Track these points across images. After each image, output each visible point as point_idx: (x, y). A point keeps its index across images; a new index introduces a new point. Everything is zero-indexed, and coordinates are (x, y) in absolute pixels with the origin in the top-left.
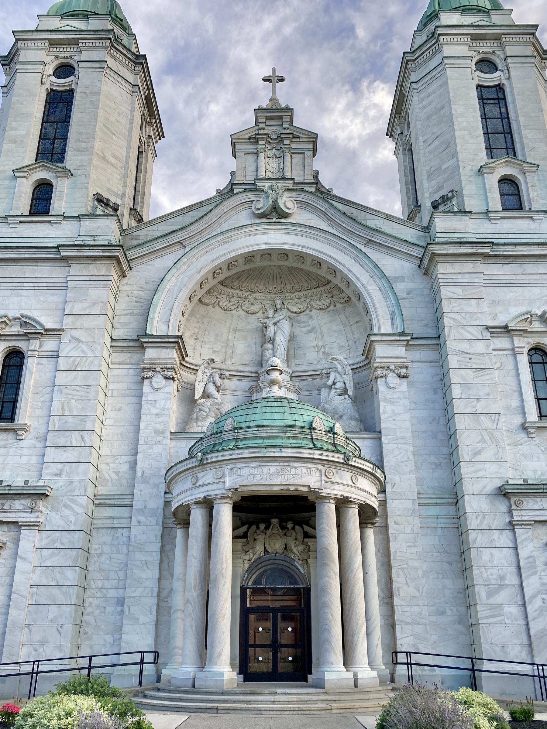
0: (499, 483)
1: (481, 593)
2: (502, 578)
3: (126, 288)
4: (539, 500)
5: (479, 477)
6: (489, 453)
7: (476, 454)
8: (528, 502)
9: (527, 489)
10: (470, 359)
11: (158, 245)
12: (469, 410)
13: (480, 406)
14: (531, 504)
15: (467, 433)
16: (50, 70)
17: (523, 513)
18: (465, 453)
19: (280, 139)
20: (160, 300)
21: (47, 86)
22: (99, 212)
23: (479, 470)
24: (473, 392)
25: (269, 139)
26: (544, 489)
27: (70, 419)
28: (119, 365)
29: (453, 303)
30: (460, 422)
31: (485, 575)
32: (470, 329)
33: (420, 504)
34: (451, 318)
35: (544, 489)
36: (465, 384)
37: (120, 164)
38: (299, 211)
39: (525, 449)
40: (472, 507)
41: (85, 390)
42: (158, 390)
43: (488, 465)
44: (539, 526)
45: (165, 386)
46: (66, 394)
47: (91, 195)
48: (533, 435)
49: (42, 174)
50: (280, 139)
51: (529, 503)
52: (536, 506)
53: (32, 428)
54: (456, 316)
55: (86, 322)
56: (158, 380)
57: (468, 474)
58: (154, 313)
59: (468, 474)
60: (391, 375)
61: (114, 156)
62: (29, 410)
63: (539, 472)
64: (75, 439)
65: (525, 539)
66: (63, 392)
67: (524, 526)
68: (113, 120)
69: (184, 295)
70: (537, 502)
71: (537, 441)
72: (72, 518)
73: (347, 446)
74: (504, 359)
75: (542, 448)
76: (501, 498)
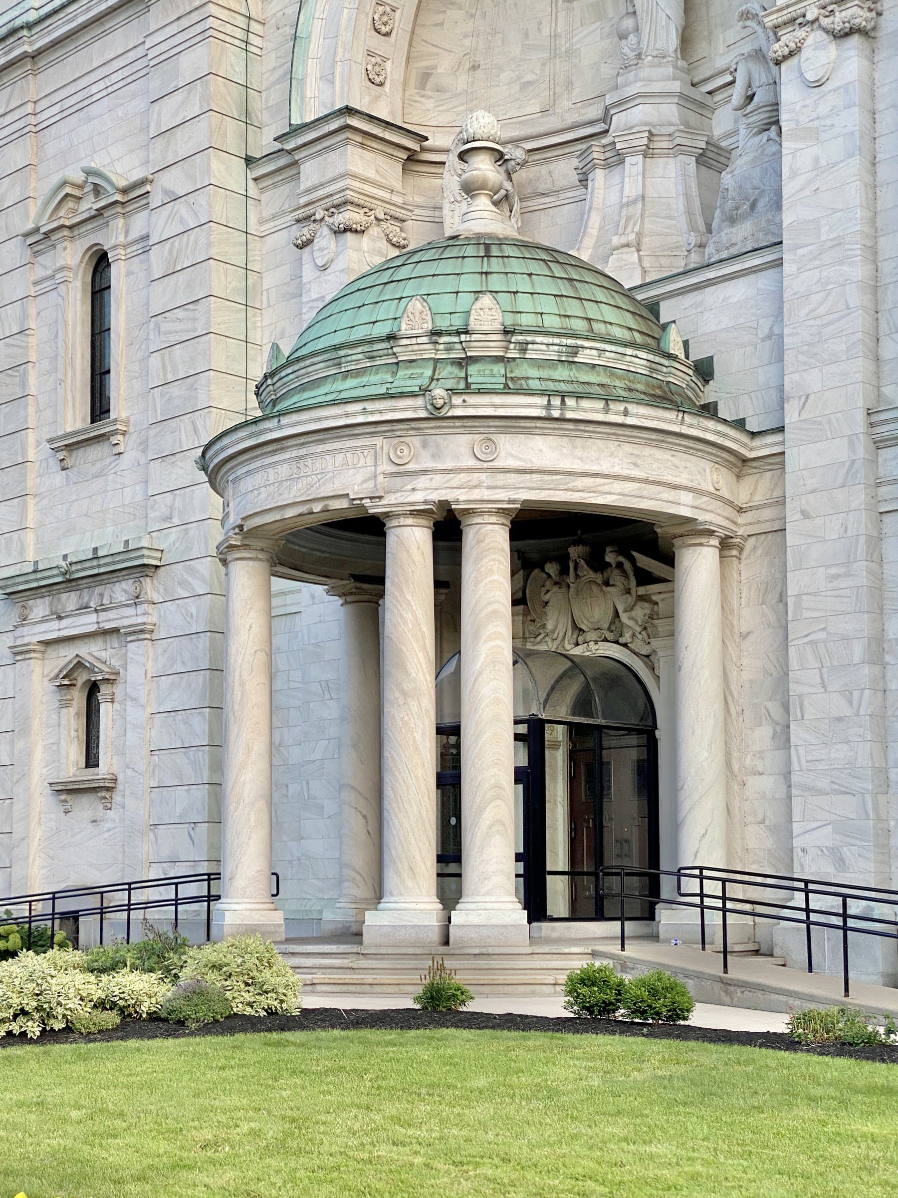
27: (175, 390)
28: (272, 224)
41: (190, 314)
42: (324, 268)
45: (337, 254)
46: (166, 333)
53: (131, 423)
56: (325, 240)
58: (305, 62)
62: (123, 386)
66: (162, 329)
73: (524, 350)
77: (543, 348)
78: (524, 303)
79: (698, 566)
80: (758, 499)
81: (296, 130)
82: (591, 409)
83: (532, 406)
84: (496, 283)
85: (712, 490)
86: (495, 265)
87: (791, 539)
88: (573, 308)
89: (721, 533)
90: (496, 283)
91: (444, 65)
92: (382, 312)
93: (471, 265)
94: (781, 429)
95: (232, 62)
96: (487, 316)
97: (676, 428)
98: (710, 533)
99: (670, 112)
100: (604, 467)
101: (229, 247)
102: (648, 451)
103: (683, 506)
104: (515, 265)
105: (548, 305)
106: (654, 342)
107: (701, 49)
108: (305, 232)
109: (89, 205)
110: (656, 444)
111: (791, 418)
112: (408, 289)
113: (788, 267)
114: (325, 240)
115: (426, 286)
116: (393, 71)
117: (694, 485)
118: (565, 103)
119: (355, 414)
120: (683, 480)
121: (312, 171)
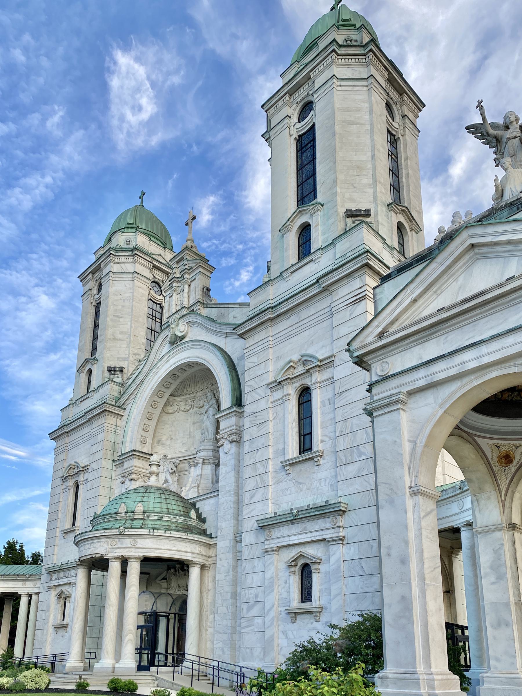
2: (256, 596)
4: (281, 528)
7: (252, 497)
8: (275, 532)
9: (269, 521)
10: (256, 417)
12: (252, 461)
13: (258, 456)
14: (276, 533)
15: (249, 480)
17: (271, 541)
23: (252, 510)
25: (178, 280)
26: (279, 519)
31: (247, 596)
32: (258, 391)
34: (248, 386)
35: (279, 519)
39: (284, 485)
40: (245, 542)
43: (258, 505)
44: (284, 550)
48: (288, 472)
51: (276, 533)
52: (279, 535)
57: (246, 514)
59: (246, 514)
63: (290, 504)
65: (270, 564)
67: (270, 553)
70: (280, 531)
75: (294, 481)
76: (261, 531)
79: (194, 572)
80: (213, 554)
85: (198, 552)
87: (218, 565)
89: (201, 564)
94: (217, 537)
97: (185, 537)
98: (197, 564)
102: (178, 543)
103: (188, 557)
110: (181, 541)
111: (219, 534)
113: (220, 496)
117: (193, 551)
120: (189, 550)
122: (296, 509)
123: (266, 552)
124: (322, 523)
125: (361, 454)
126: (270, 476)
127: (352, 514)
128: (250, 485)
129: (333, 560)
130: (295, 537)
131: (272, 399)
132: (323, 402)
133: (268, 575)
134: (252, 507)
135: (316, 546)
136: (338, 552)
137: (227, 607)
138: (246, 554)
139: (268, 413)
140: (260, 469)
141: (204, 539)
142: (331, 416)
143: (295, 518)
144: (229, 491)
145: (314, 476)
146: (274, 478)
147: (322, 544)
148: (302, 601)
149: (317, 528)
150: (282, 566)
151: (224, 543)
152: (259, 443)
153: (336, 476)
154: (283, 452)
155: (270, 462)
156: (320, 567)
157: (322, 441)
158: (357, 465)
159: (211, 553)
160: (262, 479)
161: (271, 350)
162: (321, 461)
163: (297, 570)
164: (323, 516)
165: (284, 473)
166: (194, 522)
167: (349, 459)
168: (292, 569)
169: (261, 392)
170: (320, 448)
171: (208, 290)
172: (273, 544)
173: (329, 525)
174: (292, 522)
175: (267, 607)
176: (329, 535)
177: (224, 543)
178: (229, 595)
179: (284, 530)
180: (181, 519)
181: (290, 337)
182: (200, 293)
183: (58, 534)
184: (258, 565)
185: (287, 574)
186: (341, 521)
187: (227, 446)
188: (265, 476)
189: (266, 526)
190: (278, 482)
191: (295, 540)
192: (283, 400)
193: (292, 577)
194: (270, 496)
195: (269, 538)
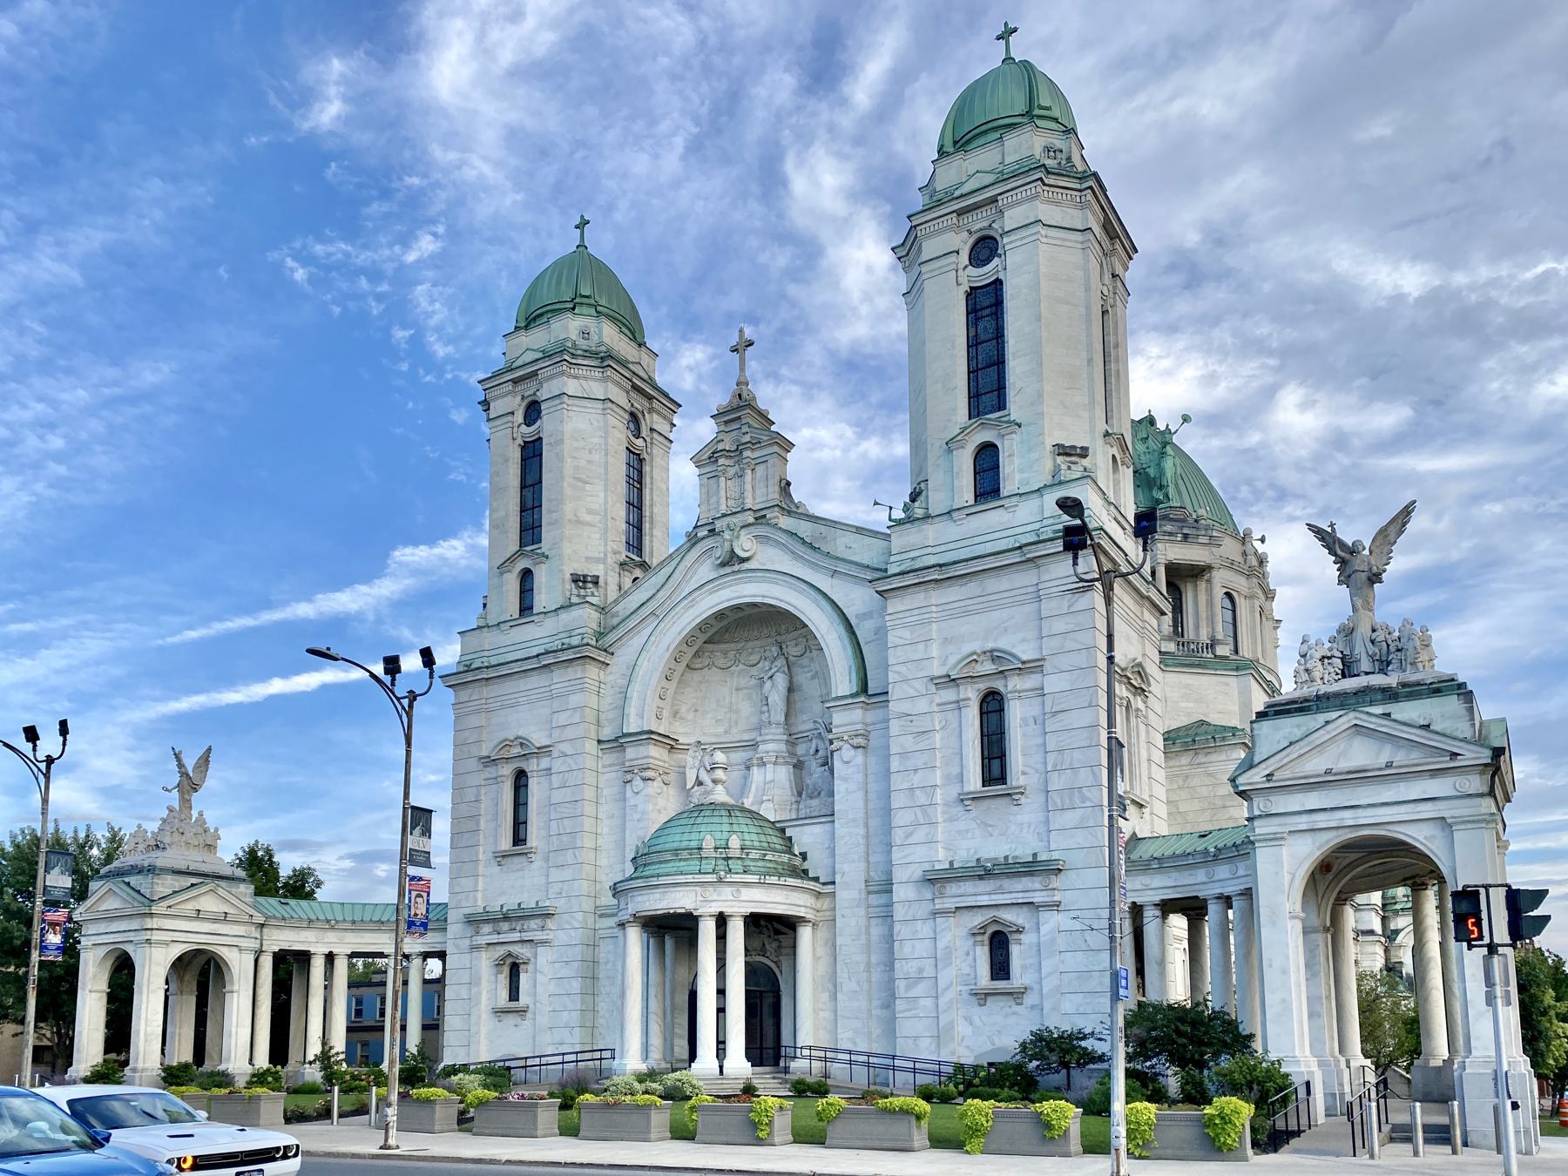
0: (927, 867)
1: (901, 985)
3: (611, 678)
5: (911, 861)
6: (920, 835)
7: (907, 837)
11: (631, 623)
12: (905, 785)
13: (917, 780)
15: (901, 813)
16: (519, 417)
18: (898, 836)
19: (739, 451)
20: (635, 692)
21: (520, 441)
22: (575, 600)
24: (910, 764)
29: (899, 651)
30: (898, 801)
32: (915, 684)
33: (869, 893)
36: (904, 755)
37: (598, 518)
38: (761, 548)
39: (961, 825)
47: (568, 577)
49: (523, 564)
50: (739, 451)
51: (952, 889)
52: (959, 892)
54: (902, 668)
55: (570, 733)
56: (638, 782)
60: (846, 746)
61: (590, 512)
64: (569, 857)
68: (583, 463)
69: (657, 675)
71: (973, 814)
72: (572, 933)
74: (950, 715)
77: (754, 854)
78: (746, 836)
81: (625, 735)
82: (774, 880)
83: (754, 878)
84: (735, 828)
86: (734, 820)
88: (763, 838)
90: (735, 828)
91: (684, 709)
92: (694, 836)
93: (725, 820)
95: (593, 701)
96: (735, 842)
99: (783, 747)
100: (778, 899)
101: (590, 778)
103: (801, 912)
104: (741, 820)
105: (754, 837)
106: (789, 850)
107: (792, 720)
108: (629, 777)
109: (516, 750)
112: (703, 828)
113: (837, 824)
114: (638, 782)
115: (713, 828)
116: (665, 713)
118: (734, 730)
119: (689, 878)
121: (631, 752)
122: (988, 860)
123: (935, 914)
124: (1026, 882)
125: (1084, 799)
126: (939, 809)
127: (1072, 875)
128: (901, 818)
129: (1044, 929)
130: (986, 897)
131: (938, 700)
132: (1024, 720)
133: (941, 944)
134: (908, 850)
135: (1015, 909)
136: (1050, 921)
137: (858, 983)
138: (899, 912)
139: (932, 720)
140: (922, 798)
141: (811, 885)
142: (1040, 741)
143: (984, 872)
144: (854, 820)
145: (1011, 818)
146: (944, 813)
147: (1025, 908)
148: (992, 979)
149: (1019, 887)
150: (963, 932)
151: (849, 893)
152: (919, 761)
153: (1047, 821)
154: (961, 778)
155: (939, 791)
156: (1022, 936)
157: (1024, 773)
158: (1079, 812)
159: (825, 904)
160: (925, 814)
161: (934, 626)
162: (1023, 800)
163: (986, 938)
164: (1030, 874)
165: (960, 808)
166: (798, 861)
167: (1067, 804)
168: (979, 938)
169: (920, 686)
170: (1021, 783)
171: (788, 484)
172: (950, 904)
173: (1038, 886)
174: (980, 877)
175: (941, 985)
176: (1038, 898)
177: (849, 893)
178: (862, 967)
179: (968, 887)
180: (785, 858)
181: (966, 613)
182: (777, 489)
183: (484, 853)
184: (925, 929)
185: (971, 942)
186: (1056, 882)
187: (847, 752)
188: (929, 810)
189: (935, 880)
190: (952, 820)
191: (984, 900)
192: (959, 705)
193: (978, 949)
194: (940, 837)
195: (942, 895)
